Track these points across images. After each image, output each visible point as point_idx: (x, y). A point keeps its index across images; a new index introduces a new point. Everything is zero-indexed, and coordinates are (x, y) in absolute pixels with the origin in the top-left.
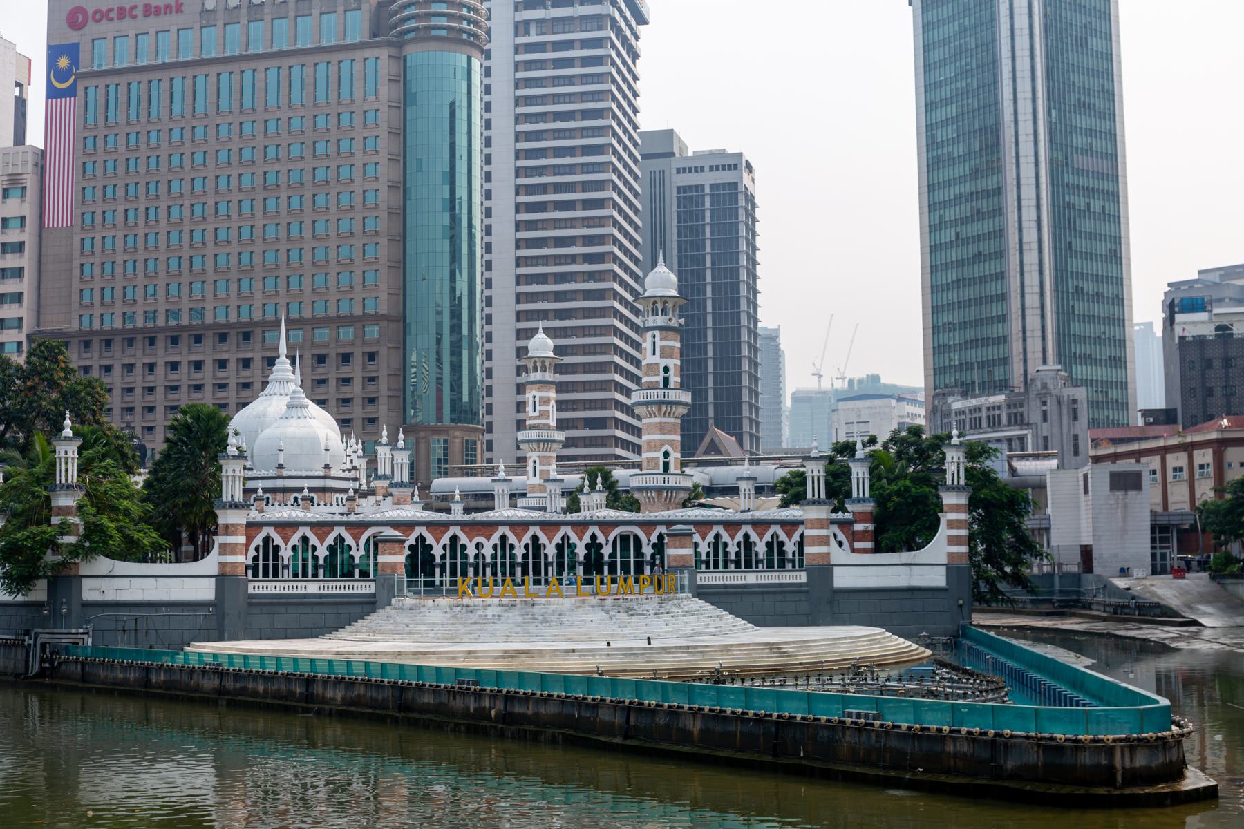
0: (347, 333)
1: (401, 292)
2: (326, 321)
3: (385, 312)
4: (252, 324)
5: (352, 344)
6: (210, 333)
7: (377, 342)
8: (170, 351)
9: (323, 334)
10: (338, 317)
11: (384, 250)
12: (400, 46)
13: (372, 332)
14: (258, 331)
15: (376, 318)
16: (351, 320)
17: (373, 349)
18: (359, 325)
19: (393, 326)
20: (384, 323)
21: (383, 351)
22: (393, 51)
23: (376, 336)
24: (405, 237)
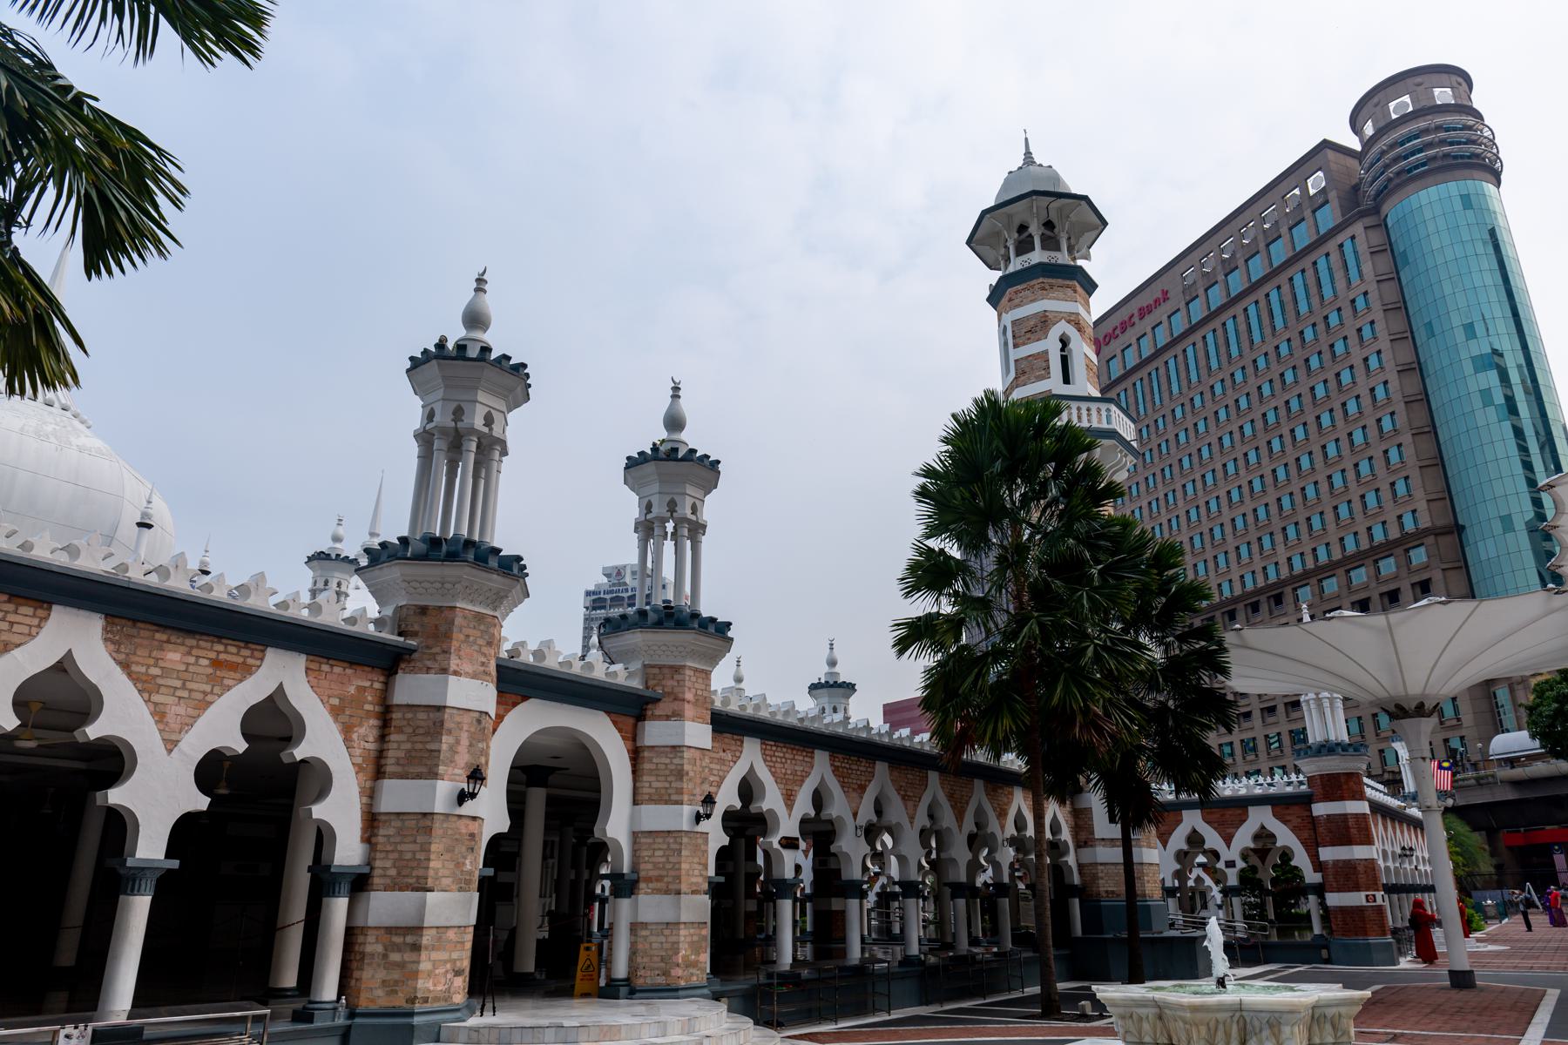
0: (1388, 566)
1: (1446, 495)
2: (1357, 559)
3: (1428, 525)
4: (1281, 583)
5: (1396, 577)
6: (1240, 606)
7: (1426, 567)
8: (1276, 613)
9: (1360, 576)
10: (1372, 548)
11: (1409, 452)
12: (1376, 210)
13: (1419, 556)
14: (1288, 590)
15: (1418, 537)
16: (1387, 548)
17: (1425, 576)
18: (1399, 551)
19: (1445, 541)
20: (1430, 540)
21: (1437, 576)
22: (1369, 221)
23: (1425, 559)
24: (1434, 427)
